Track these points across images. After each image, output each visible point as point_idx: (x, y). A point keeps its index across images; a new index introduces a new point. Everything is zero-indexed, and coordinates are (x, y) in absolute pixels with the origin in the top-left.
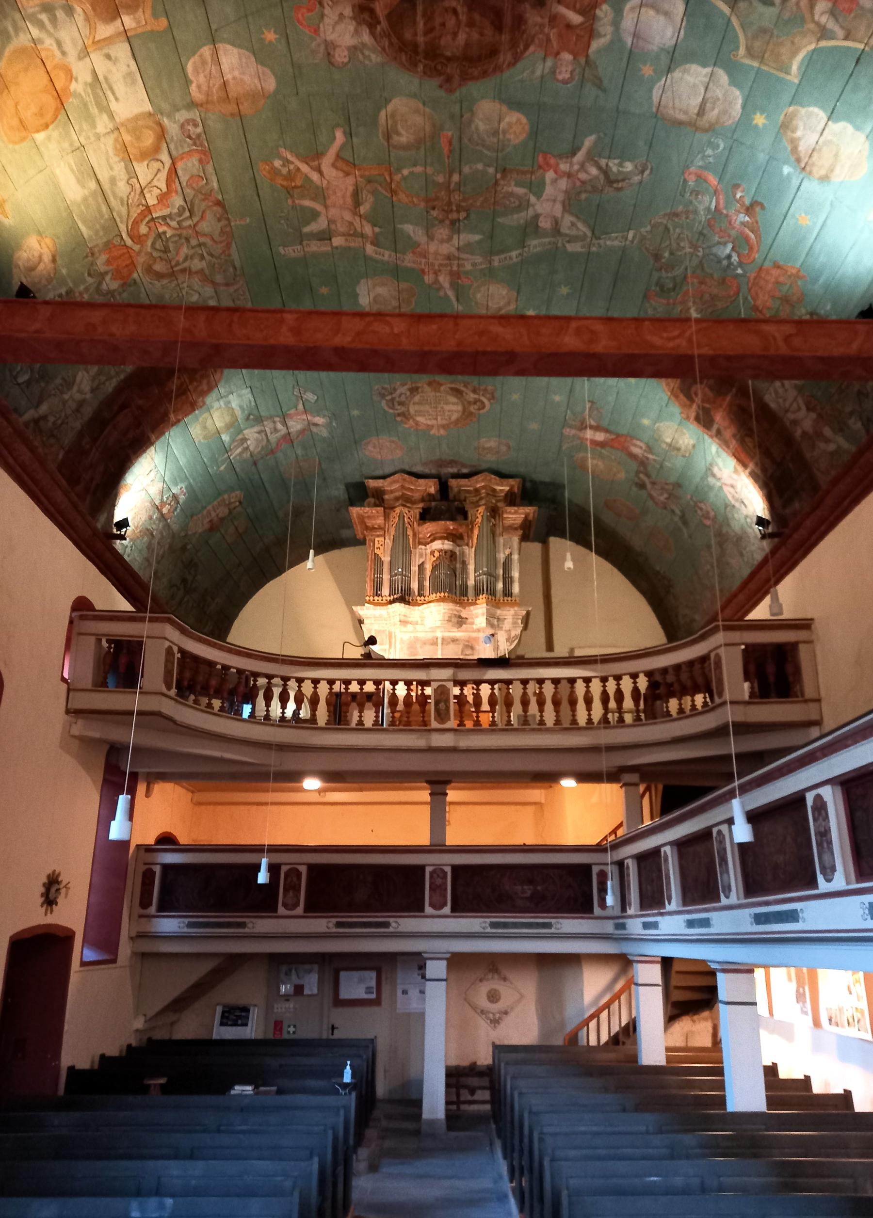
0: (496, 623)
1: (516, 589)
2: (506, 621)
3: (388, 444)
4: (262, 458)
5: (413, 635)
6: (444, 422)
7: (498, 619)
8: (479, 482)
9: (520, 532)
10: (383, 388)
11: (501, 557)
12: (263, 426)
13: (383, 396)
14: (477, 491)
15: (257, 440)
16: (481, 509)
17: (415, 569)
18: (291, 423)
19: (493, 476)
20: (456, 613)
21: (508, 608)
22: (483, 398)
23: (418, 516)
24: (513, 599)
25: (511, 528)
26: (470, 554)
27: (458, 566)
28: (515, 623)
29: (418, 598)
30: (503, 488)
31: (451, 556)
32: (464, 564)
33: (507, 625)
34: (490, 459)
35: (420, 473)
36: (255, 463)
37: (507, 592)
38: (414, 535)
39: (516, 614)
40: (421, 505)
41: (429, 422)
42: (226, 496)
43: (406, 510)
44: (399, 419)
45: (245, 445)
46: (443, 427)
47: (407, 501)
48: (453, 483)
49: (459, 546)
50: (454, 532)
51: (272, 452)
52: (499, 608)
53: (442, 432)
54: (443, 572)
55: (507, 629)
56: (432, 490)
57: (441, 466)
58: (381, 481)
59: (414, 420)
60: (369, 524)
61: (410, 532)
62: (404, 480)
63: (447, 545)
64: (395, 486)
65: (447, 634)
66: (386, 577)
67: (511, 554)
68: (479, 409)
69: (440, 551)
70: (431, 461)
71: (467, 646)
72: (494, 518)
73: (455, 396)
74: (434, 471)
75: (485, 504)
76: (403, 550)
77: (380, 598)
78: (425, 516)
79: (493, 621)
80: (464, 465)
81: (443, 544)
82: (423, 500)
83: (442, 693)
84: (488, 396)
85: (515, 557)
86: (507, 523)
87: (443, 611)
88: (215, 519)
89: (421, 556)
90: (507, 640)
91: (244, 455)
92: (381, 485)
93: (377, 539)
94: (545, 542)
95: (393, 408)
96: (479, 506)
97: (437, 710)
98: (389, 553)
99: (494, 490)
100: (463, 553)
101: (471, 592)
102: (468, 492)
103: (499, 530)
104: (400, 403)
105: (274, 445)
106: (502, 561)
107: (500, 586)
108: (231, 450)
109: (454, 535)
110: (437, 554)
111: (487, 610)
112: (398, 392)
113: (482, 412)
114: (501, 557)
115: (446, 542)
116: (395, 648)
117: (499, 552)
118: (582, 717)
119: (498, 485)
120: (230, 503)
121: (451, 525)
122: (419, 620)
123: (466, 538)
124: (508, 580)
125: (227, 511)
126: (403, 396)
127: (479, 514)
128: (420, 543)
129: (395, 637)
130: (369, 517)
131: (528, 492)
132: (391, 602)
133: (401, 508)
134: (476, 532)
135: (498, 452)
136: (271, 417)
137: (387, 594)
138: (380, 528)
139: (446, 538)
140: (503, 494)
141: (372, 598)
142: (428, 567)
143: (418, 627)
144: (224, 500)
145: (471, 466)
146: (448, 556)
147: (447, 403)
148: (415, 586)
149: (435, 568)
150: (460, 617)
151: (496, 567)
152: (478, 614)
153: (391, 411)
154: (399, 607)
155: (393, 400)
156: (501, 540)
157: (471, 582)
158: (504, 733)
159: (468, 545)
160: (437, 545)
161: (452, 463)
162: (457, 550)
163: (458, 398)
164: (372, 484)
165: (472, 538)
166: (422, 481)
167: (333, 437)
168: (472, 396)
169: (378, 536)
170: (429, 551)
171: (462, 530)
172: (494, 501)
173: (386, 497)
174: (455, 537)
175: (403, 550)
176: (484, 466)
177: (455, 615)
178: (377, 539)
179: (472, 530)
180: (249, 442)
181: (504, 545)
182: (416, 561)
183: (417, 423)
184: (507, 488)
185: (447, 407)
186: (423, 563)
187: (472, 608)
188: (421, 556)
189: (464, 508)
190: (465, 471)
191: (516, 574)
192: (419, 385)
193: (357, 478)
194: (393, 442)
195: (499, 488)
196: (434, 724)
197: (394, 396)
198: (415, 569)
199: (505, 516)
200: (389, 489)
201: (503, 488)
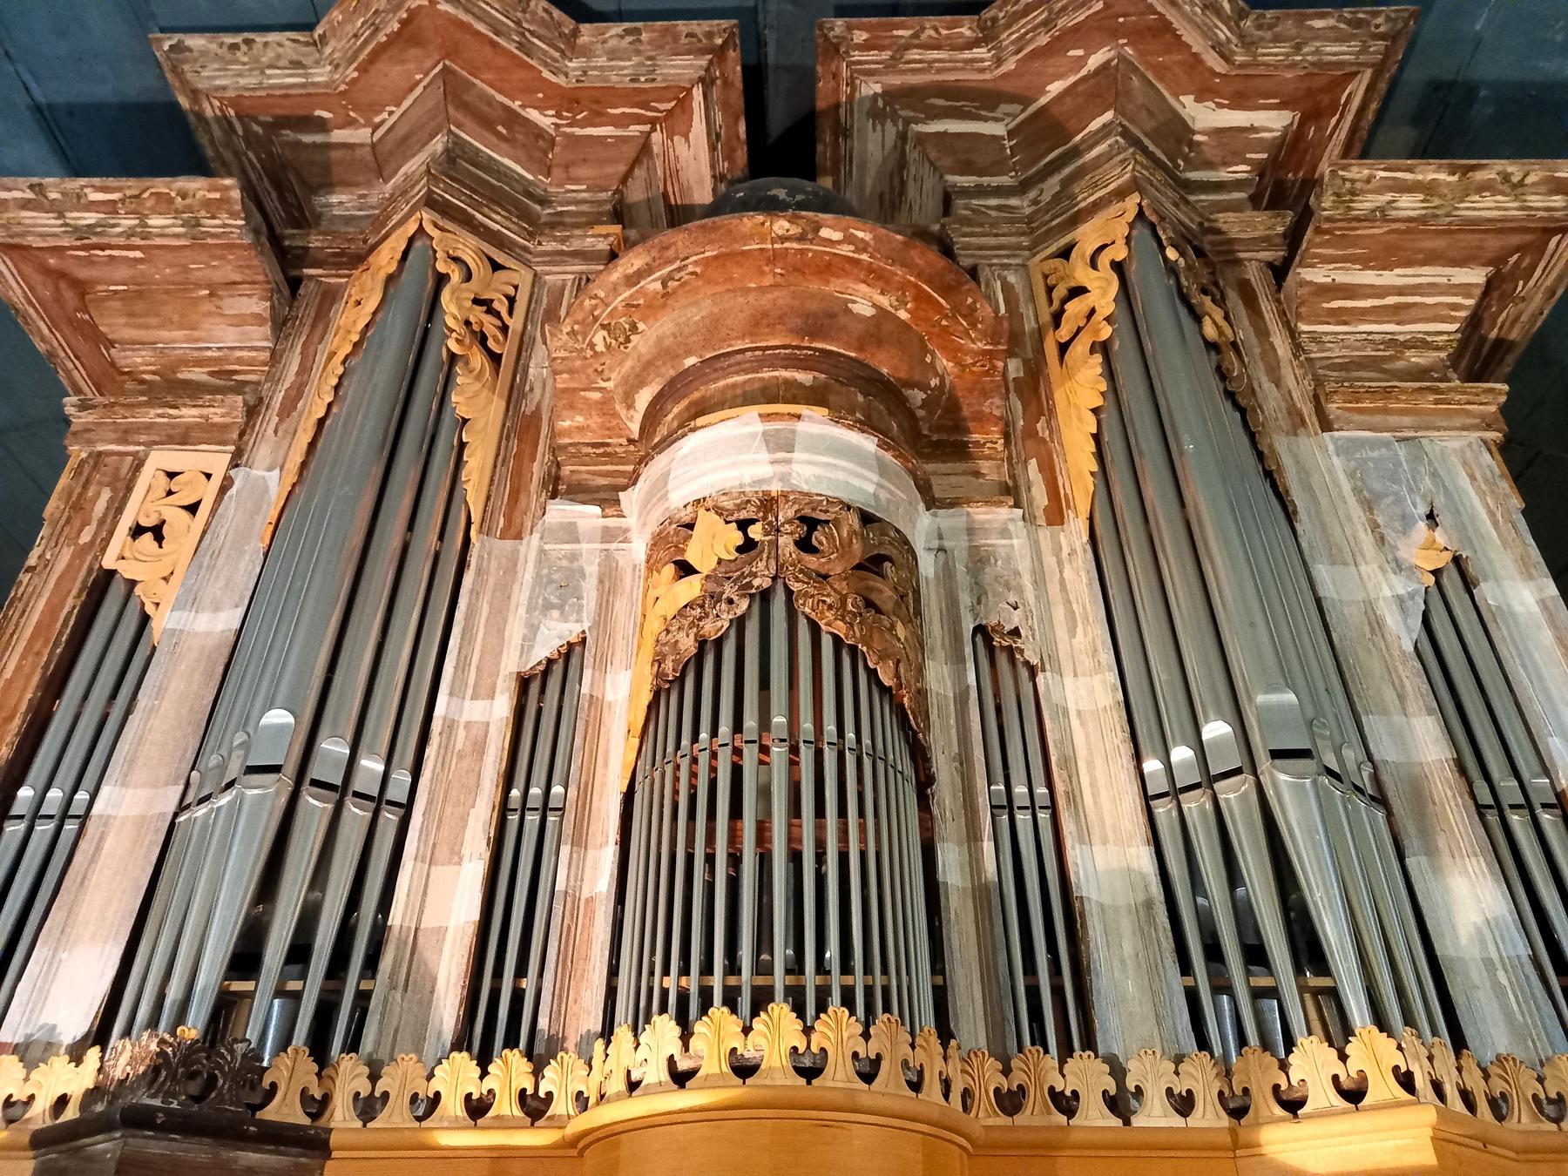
17: (477, 713)
25: (1377, 378)
26: (1044, 572)
29: (457, 1077)
31: (873, 564)
38: (521, 426)
43: (468, 247)
49: (931, 503)
54: (780, 736)
60: (139, 360)
61: (476, 402)
63: (832, 460)
69: (751, 514)
75: (1135, 186)
81: (782, 444)
86: (1336, 338)
89: (560, 589)
92: (281, 78)
96: (1075, 221)
98: (247, 567)
99: (1177, 132)
101: (1131, 983)
102: (967, 153)
103: (1281, 389)
106: (1403, 632)
110: (712, 545)
115: (814, 423)
123: (987, 438)
128: (555, 487)
133: (427, 216)
134: (1079, 391)
137: (75, 1020)
138: (226, 381)
142: (619, 692)
148: (442, 903)
149: (680, 688)
159: (1011, 492)
160: (724, 458)
162: (921, 527)
169: (183, 437)
175: (390, 546)
179: (1034, 389)
184: (1273, 121)
186: (570, 654)
195: (1205, 116)
198: (477, 713)
200: (362, 135)
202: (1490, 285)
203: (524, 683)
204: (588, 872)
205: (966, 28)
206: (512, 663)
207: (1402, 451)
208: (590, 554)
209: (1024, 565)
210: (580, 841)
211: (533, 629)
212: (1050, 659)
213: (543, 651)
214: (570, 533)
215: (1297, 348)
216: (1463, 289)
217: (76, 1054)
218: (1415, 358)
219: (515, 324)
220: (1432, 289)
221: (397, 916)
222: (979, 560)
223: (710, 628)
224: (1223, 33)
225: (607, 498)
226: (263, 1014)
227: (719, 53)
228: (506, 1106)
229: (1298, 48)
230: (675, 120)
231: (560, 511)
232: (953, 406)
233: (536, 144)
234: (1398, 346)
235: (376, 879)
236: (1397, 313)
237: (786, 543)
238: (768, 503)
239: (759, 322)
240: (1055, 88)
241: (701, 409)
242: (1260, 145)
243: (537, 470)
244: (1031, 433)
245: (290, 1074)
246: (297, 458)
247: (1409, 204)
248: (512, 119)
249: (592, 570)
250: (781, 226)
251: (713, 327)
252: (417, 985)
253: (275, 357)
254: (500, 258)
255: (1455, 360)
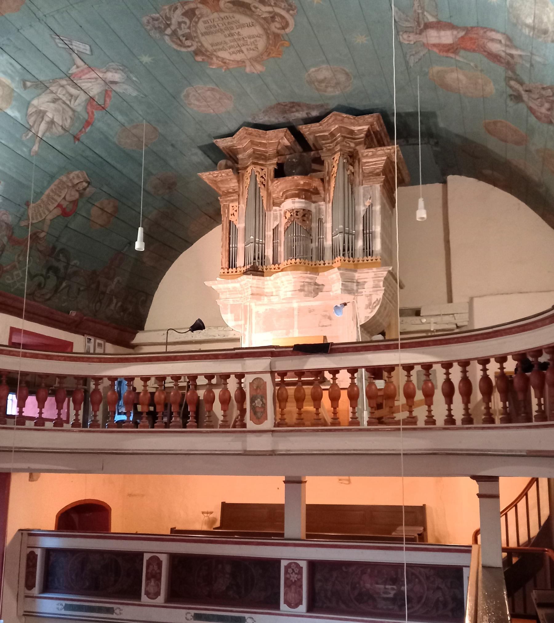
0: (355, 288)
1: (377, 246)
2: (366, 286)
3: (209, 93)
4: (80, 131)
5: (268, 307)
6: (253, 54)
7: (358, 283)
8: (332, 124)
9: (382, 178)
10: (154, 19)
11: (361, 209)
12: (52, 92)
13: (161, 31)
14: (332, 134)
15: (56, 110)
16: (337, 156)
17: (269, 233)
18: (85, 85)
19: (345, 115)
20: (308, 280)
21: (366, 270)
22: (277, 10)
23: (272, 174)
24: (374, 258)
27: (314, 225)
28: (376, 286)
29: (273, 266)
30: (361, 127)
31: (304, 216)
32: (320, 221)
33: (368, 288)
34: (334, 95)
35: (268, 123)
36: (76, 138)
37: (368, 251)
38: (269, 195)
39: (376, 277)
40: (275, 161)
41: (239, 57)
42: (64, 179)
43: (258, 168)
44: (199, 58)
45: (47, 119)
46: (256, 60)
47: (259, 158)
48: (305, 129)
49: (314, 202)
50: (306, 188)
51: (88, 123)
52: (356, 271)
53: (259, 68)
55: (368, 293)
56: (286, 142)
57: (284, 112)
58: (229, 139)
59: (218, 57)
61: (263, 193)
62: (250, 134)
64: (246, 143)
65: (303, 304)
66: (241, 246)
67: (371, 205)
68: (283, 28)
70: (272, 108)
71: (325, 316)
72: (352, 165)
73: (246, 14)
74: (281, 120)
76: (258, 214)
77: (234, 269)
78: (280, 172)
79: (351, 287)
80: (309, 107)
81: (294, 203)
82: (278, 154)
83: (258, 386)
84: (283, 5)
85: (377, 208)
86: (367, 169)
87: (293, 280)
88: (65, 204)
89: (275, 218)
90: (368, 306)
91: (54, 130)
93: (231, 205)
94: (445, 182)
95: (182, 45)
97: (253, 408)
98: (243, 218)
99: (352, 132)
100: (319, 211)
101: (328, 254)
104: (188, 37)
105: (86, 116)
107: (360, 244)
108: (31, 127)
109: (307, 191)
110: (288, 215)
111: (342, 275)
112: (174, 21)
113: (288, 30)
114: (361, 209)
115: (297, 200)
116: (251, 323)
117: (359, 205)
118: (421, 413)
119: (353, 124)
120: (74, 186)
121: (300, 180)
122: (274, 290)
123: (322, 192)
124: (368, 237)
125: (77, 195)
126: (183, 25)
127: (335, 163)
128: (275, 204)
129: (251, 310)
130: (222, 181)
131: (394, 128)
132: (245, 273)
135: (338, 84)
136: (54, 81)
139: (298, 196)
140: (363, 135)
141: (226, 271)
142: (282, 229)
143: (274, 299)
144: (62, 182)
145: (322, 106)
146: (299, 217)
147: (242, 26)
148: (269, 253)
150: (316, 284)
151: (355, 222)
152: (332, 278)
153: (183, 50)
154: (250, 280)
155: (174, 32)
156: (361, 190)
157: (328, 243)
158: (326, 433)
159: (324, 200)
161: (295, 106)
162: (313, 207)
163: (251, 16)
164: (222, 143)
165: (329, 191)
166: (270, 133)
167: (146, 96)
168: (264, 10)
170: (282, 213)
171: (316, 183)
172: (352, 145)
173: (240, 156)
174: (308, 194)
175: (258, 214)
176: (333, 104)
177: (309, 283)
178: (231, 205)
180: (50, 115)
181: (364, 196)
182: (271, 224)
183: (223, 61)
185: (245, 32)
187: (326, 273)
188: (275, 218)
189: (320, 157)
190: (315, 113)
191: (377, 229)
192: (192, 6)
193: (207, 141)
194: (213, 90)
195: (356, 128)
196: (250, 425)
197: (173, 27)
198: (269, 233)
199: (364, 160)
201: (361, 127)
202: (388, 158)
203: (273, 230)
204: (281, 249)
205: (318, 124)
206: (272, 228)
207: (370, 188)
208: (278, 212)
209: (324, 209)
210: (280, 246)
211: (273, 223)
212: (326, 222)
213: (275, 226)
214: (276, 211)
215: (362, 171)
216: (383, 160)
217: (244, 267)
218: (378, 171)
219: (266, 178)
220: (379, 161)
221: (266, 254)
222: (320, 209)
223: (288, 225)
224: (353, 121)
225: (279, 207)
226: (257, 264)
227: (286, 132)
228: (277, 268)
229: (364, 121)
230: (282, 138)
231: (274, 208)
232: (317, 189)
233: (264, 145)
234: (375, 169)
235: (263, 251)
236: (375, 164)
237: (295, 215)
238: (293, 210)
239: (291, 187)
240: (333, 129)
241: (286, 198)
242: (364, 131)
243: (272, 201)
244: (328, 189)
245: (260, 267)
246: (245, 204)
247: (370, 154)
248: (261, 143)
249: (279, 215)
250: (290, 178)
251: (286, 187)
252: (268, 259)
253: (239, 187)
254: (263, 168)
255: (382, 171)
